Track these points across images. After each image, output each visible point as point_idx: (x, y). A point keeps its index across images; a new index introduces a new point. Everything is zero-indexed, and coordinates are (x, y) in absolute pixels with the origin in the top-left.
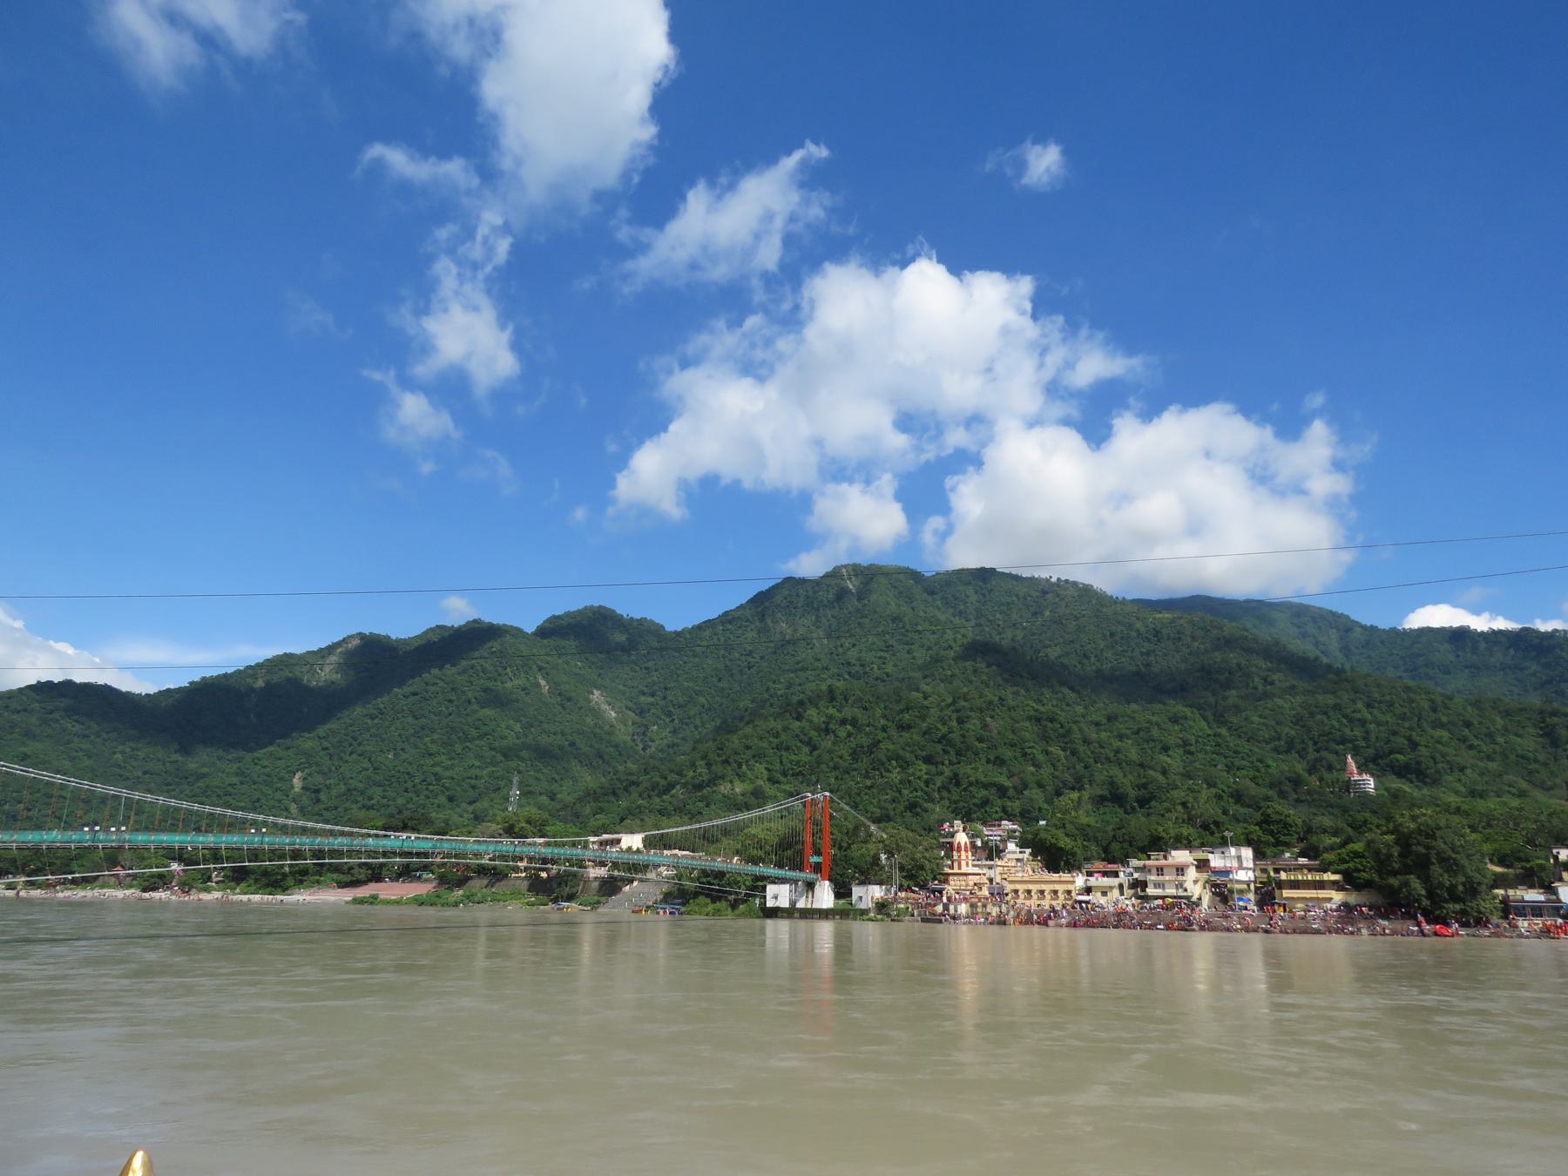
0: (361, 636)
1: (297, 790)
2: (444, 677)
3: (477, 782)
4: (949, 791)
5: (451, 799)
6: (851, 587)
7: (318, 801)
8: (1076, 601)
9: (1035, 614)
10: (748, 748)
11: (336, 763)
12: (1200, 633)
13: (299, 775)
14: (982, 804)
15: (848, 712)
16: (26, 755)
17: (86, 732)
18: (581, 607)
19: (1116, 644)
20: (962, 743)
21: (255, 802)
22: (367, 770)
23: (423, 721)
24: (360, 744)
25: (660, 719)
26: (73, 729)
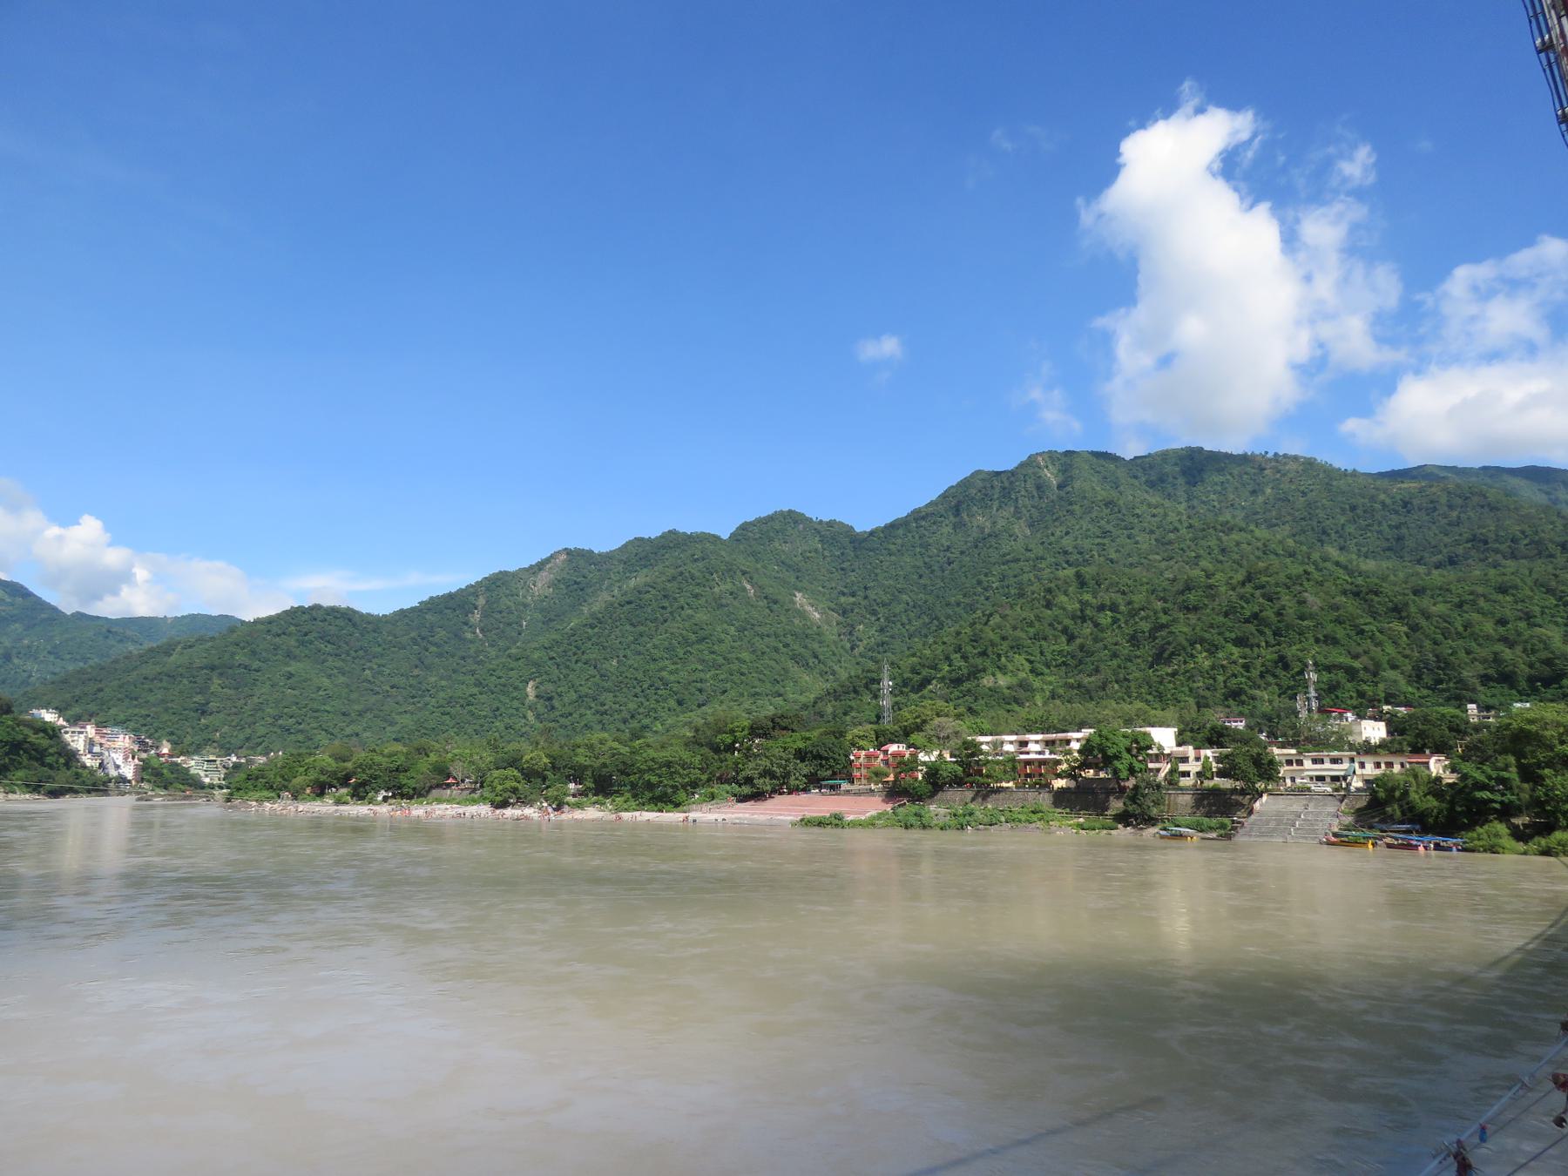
0: (568, 552)
1: (531, 698)
2: (655, 585)
3: (703, 686)
4: (1275, 676)
5: (680, 703)
6: (1049, 475)
7: (553, 708)
8: (1300, 476)
9: (1254, 492)
10: (1004, 638)
11: (563, 671)
12: (1459, 501)
13: (531, 684)
14: (1329, 688)
15: (1106, 598)
16: (291, 674)
17: (338, 652)
18: (770, 512)
19: (1359, 518)
20: (1279, 621)
21: (495, 711)
22: (594, 677)
23: (641, 628)
24: (583, 653)
25: (866, 618)
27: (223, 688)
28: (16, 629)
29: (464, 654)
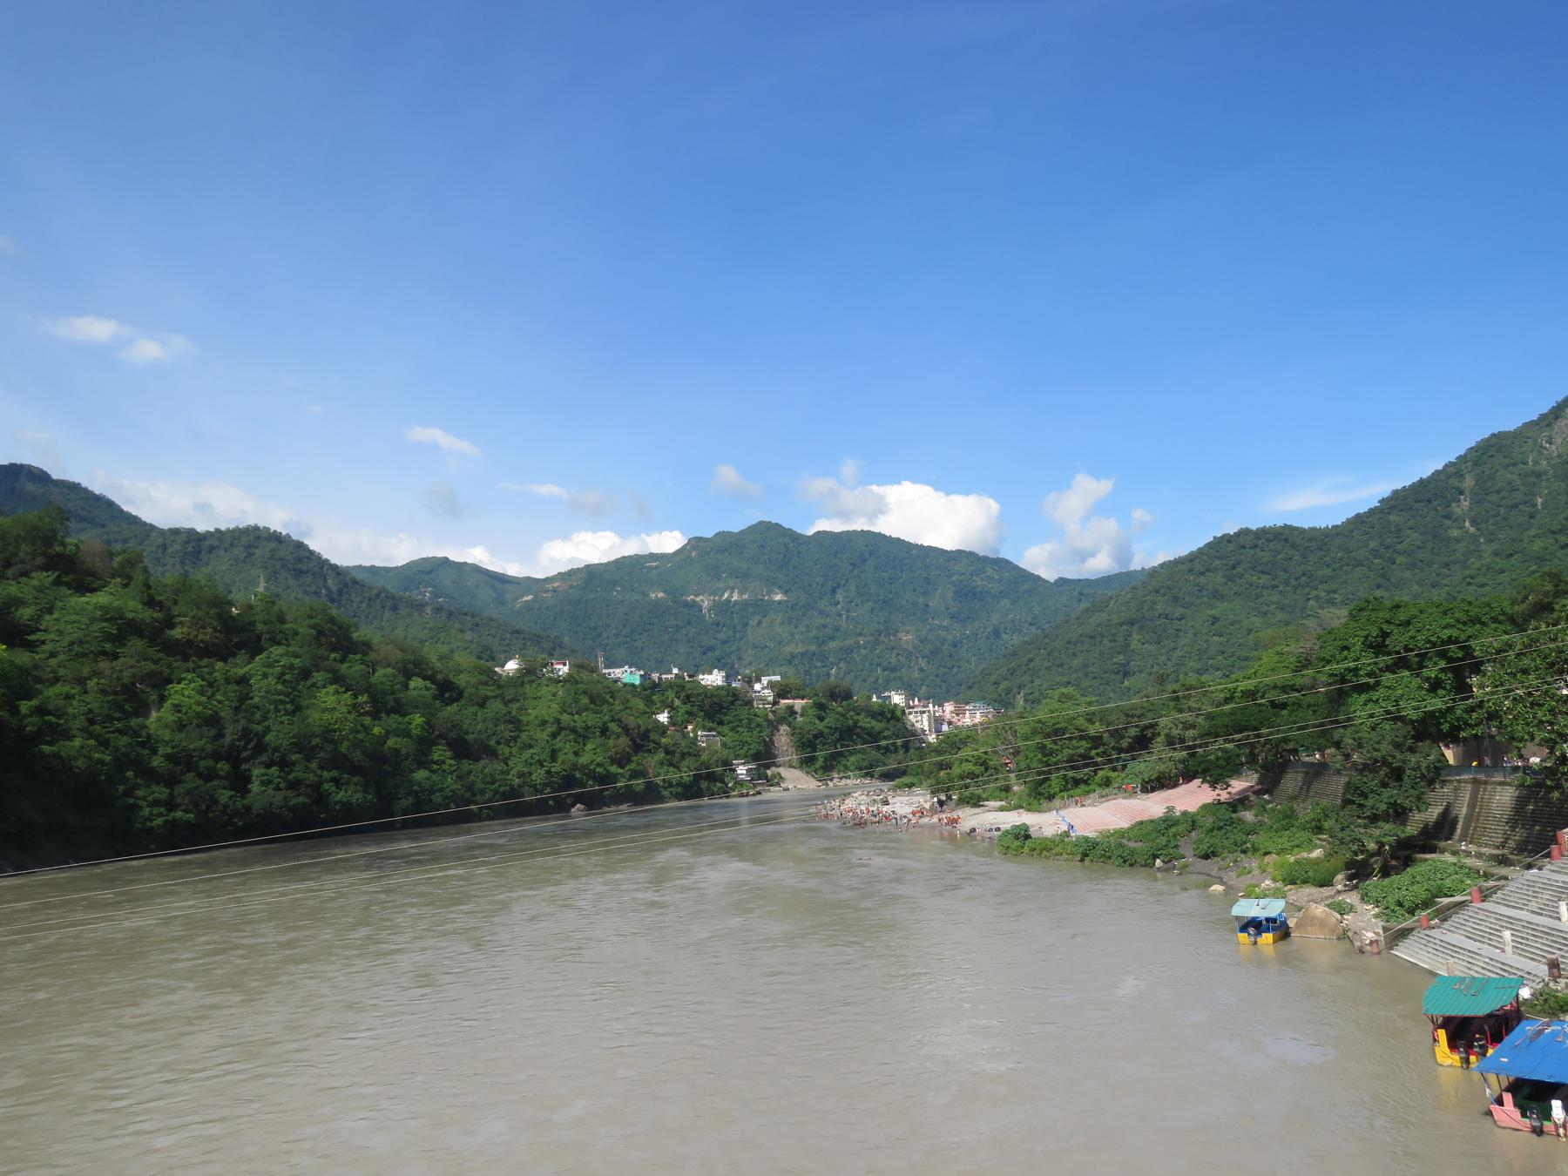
16: (1215, 618)
17: (1273, 583)
26: (1259, 581)
27: (1143, 644)
28: (1005, 605)
29: (1447, 560)
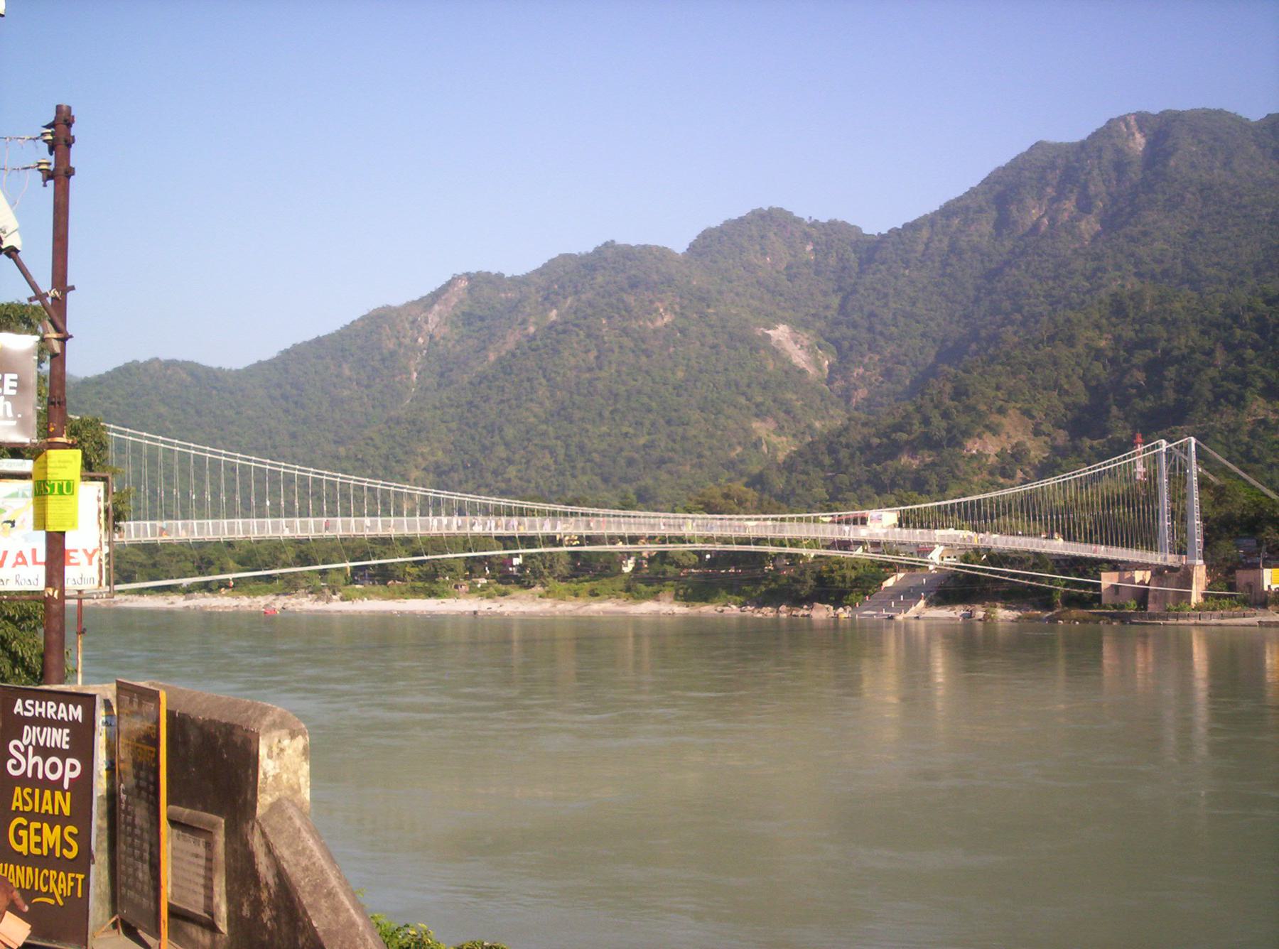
0: (469, 276)
